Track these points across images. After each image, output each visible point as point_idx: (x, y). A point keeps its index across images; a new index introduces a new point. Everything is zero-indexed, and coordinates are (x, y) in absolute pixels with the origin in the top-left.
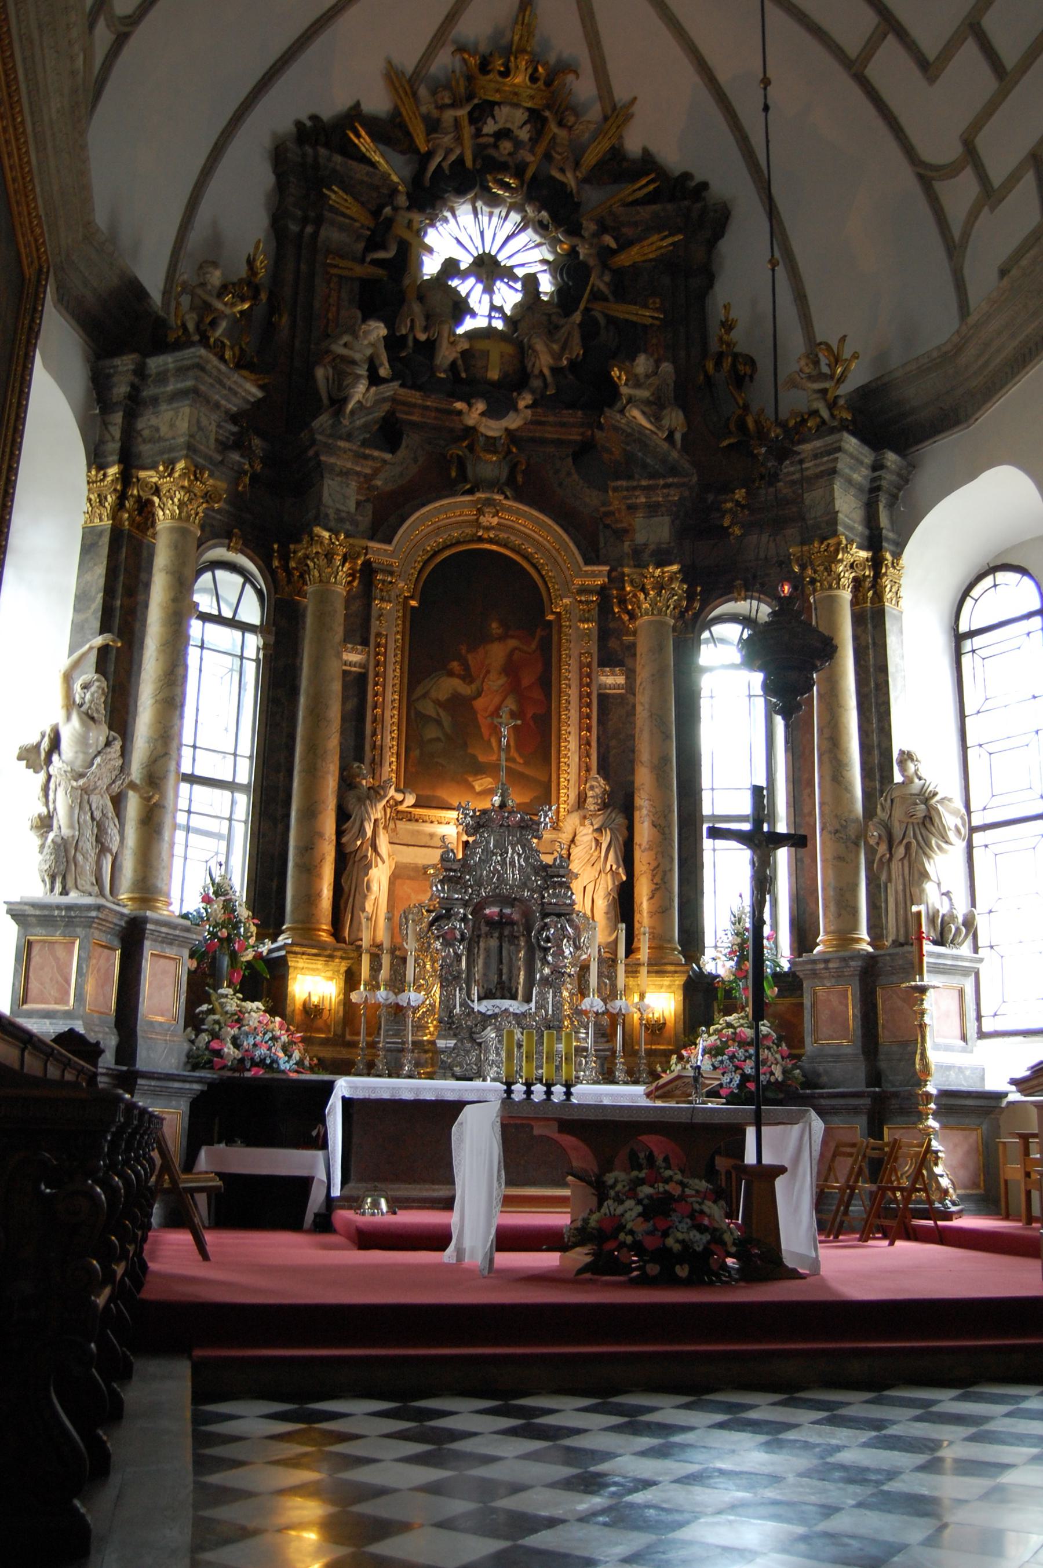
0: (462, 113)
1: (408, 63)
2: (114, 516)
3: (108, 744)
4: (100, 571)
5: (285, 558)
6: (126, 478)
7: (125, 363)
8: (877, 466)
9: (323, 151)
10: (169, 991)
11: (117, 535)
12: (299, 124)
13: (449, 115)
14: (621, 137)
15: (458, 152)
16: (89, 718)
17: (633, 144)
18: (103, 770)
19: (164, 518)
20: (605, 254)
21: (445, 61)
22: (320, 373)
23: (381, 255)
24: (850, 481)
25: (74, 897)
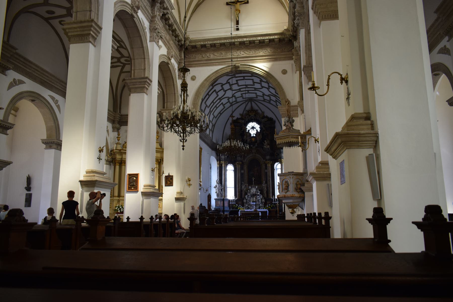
0: (248, 116)
1: (242, 113)
2: (219, 166)
3: (220, 186)
4: (219, 170)
5: (235, 164)
6: (220, 162)
10: (227, 204)
11: (220, 167)
13: (247, 116)
14: (264, 114)
15: (248, 119)
16: (218, 184)
17: (265, 115)
18: (220, 188)
19: (223, 165)
20: (264, 126)
21: (245, 112)
23: (242, 131)
25: (219, 198)
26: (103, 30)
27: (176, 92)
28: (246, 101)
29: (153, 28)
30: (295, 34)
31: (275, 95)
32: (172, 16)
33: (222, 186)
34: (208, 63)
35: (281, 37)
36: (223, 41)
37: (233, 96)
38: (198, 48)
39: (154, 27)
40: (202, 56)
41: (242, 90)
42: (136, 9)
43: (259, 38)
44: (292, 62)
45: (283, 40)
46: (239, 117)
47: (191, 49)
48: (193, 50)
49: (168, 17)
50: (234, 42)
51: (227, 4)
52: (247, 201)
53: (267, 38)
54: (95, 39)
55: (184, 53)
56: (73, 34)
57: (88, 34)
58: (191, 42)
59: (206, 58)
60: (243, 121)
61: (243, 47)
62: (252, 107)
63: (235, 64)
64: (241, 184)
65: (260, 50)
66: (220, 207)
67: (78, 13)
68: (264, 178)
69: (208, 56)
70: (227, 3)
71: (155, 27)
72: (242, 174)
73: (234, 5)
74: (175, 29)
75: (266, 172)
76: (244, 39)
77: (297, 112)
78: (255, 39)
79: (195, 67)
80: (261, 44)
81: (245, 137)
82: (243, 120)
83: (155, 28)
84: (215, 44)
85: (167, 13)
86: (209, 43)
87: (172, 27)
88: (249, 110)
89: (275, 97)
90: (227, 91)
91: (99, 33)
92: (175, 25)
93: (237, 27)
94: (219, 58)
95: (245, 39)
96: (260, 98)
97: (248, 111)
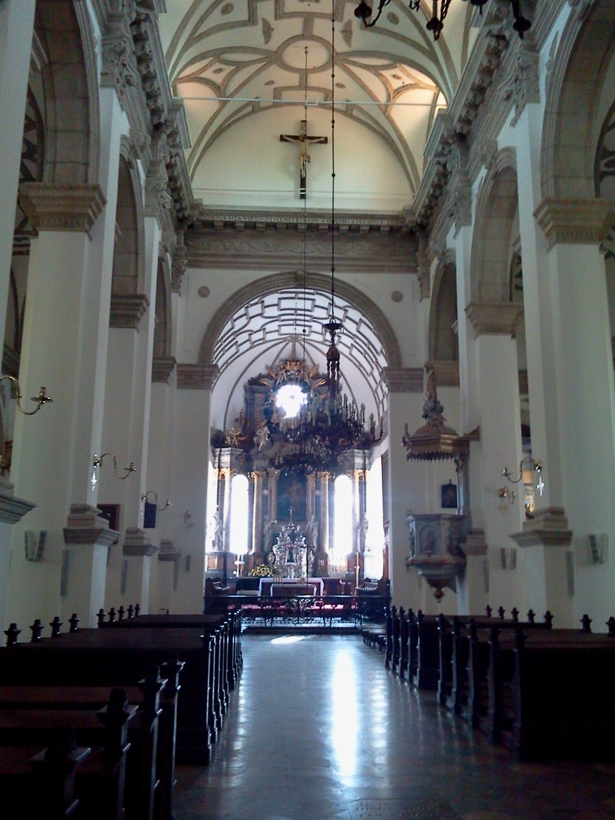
0: (283, 372)
1: (270, 364)
6: (219, 470)
7: (218, 450)
8: (364, 453)
9: (254, 386)
12: (249, 380)
13: (281, 372)
14: (317, 370)
21: (277, 363)
22: (255, 439)
23: (268, 403)
24: (358, 456)
26: (108, 205)
27: (168, 320)
28: (285, 340)
29: (154, 188)
30: (425, 221)
31: (355, 335)
32: (181, 160)
33: (222, 523)
34: (237, 262)
35: (395, 224)
36: (273, 220)
37: (263, 329)
38: (216, 228)
39: (157, 185)
40: (224, 245)
41: (283, 318)
42: (139, 152)
43: (350, 222)
44: (414, 277)
45: (399, 229)
46: (264, 372)
47: (201, 227)
48: (206, 230)
49: (175, 161)
50: (296, 224)
51: (282, 139)
52: (275, 558)
53: (366, 222)
54: (91, 223)
55: (185, 236)
56: (47, 210)
57: (81, 214)
58: (201, 214)
59: (232, 252)
60: (272, 382)
61: (313, 235)
62: (294, 350)
63: (295, 270)
64: (263, 520)
65: (350, 245)
66: (217, 572)
67: (58, 165)
68: (312, 507)
69: (237, 247)
70: (281, 136)
71: (160, 187)
72: (265, 498)
73: (298, 144)
74: (181, 185)
75: (316, 496)
76: (319, 220)
77: (420, 381)
78: (341, 223)
79: (207, 267)
80: (352, 234)
81: (275, 416)
82: (271, 380)
83: (160, 189)
84: (255, 223)
85: (177, 155)
86: (243, 220)
87: (176, 182)
88: (287, 360)
89: (352, 338)
90: (253, 319)
91: (100, 210)
92: (182, 177)
93: (301, 191)
94: (261, 253)
95: (320, 221)
96: (314, 337)
97: (286, 361)
